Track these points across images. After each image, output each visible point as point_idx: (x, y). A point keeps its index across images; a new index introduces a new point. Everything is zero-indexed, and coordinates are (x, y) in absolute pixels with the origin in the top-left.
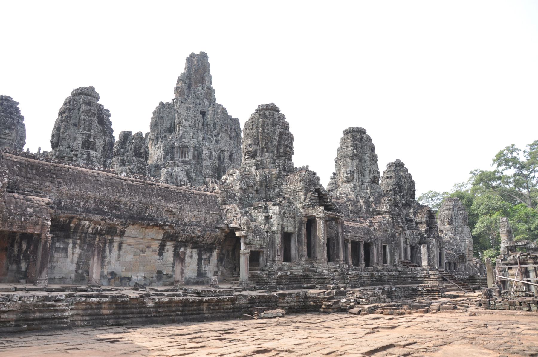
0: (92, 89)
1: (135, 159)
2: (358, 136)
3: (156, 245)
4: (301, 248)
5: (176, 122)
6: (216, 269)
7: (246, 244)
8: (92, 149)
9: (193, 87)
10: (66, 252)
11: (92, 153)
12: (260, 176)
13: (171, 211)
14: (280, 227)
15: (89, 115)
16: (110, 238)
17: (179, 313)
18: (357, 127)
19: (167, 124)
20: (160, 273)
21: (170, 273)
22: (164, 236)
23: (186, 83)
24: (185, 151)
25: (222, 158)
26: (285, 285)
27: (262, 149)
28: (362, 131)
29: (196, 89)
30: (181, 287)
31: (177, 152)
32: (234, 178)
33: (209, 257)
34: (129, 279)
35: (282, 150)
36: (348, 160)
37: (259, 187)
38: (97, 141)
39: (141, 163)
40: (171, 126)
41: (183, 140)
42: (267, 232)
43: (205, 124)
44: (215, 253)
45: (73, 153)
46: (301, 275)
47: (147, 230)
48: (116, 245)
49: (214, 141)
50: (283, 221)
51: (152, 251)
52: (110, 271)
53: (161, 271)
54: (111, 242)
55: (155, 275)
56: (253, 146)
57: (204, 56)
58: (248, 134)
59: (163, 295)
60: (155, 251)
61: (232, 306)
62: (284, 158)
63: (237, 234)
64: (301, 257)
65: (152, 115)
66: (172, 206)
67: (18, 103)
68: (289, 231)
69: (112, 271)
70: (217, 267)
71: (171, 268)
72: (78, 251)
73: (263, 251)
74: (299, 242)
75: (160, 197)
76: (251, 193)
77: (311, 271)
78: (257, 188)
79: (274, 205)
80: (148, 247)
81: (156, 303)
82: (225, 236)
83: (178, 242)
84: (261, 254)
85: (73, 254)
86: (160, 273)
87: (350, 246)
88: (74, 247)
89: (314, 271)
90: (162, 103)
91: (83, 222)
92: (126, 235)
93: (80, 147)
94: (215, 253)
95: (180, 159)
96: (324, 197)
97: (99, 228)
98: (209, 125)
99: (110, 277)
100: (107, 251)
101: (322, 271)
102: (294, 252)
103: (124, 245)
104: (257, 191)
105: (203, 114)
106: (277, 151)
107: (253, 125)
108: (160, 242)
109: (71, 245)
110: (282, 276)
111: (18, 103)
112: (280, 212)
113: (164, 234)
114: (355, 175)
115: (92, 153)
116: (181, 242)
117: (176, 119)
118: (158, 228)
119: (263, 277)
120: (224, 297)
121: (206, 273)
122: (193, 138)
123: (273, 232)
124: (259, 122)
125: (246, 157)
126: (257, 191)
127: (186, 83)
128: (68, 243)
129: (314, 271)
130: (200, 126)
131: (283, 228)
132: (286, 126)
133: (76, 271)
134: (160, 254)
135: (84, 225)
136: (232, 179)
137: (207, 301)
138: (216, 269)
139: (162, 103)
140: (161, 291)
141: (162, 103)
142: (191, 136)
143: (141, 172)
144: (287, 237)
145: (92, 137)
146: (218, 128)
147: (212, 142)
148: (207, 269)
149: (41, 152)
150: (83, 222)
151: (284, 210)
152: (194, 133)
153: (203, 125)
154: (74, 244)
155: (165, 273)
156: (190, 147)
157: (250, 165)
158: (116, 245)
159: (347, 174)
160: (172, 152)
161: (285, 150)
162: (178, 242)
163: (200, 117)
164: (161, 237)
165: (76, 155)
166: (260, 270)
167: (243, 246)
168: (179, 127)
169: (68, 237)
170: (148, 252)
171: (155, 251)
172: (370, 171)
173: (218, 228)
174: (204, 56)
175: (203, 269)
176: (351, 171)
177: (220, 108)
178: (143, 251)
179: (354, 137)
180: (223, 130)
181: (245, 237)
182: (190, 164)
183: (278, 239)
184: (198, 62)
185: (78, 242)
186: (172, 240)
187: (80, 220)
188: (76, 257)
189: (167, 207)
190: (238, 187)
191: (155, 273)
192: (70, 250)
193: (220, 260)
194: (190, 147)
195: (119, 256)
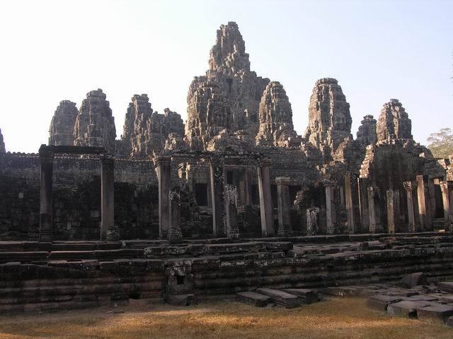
8: (98, 136)
14: (191, 181)
18: (324, 79)
28: (333, 82)
49: (238, 105)
57: (233, 26)
67: (75, 104)
111: (75, 104)
141: (196, 77)
146: (241, 93)
174: (233, 26)
184: (226, 33)
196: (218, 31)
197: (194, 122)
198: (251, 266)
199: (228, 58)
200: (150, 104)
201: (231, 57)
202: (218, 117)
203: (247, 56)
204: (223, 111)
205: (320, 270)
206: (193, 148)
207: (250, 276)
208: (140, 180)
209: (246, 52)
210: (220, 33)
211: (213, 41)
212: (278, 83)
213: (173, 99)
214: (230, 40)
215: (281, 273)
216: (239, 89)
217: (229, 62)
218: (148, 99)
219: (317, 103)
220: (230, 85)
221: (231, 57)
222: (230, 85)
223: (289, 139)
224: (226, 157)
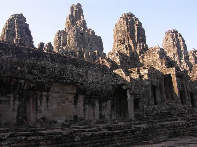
0: (22, 15)
2: (175, 35)
3: (72, 98)
4: (162, 96)
5: (68, 40)
6: (110, 113)
7: (131, 94)
10: (9, 104)
12: (130, 54)
13: (80, 74)
14: (150, 82)
16: (40, 93)
17: (99, 144)
20: (76, 117)
21: (83, 116)
22: (76, 91)
25: (94, 57)
26: (158, 119)
30: (94, 125)
32: (114, 55)
33: (106, 105)
34: (55, 122)
36: (171, 48)
37: (130, 60)
40: (65, 42)
42: (142, 86)
43: (84, 39)
44: (109, 103)
46: (166, 113)
47: (65, 87)
48: (44, 98)
49: (89, 48)
50: (151, 78)
51: (70, 102)
52: (41, 117)
53: (76, 116)
54: (41, 96)
55: (73, 119)
57: (79, 5)
58: (118, 31)
59: (85, 131)
60: (71, 102)
61: (133, 136)
63: (124, 87)
64: (163, 101)
66: (81, 71)
68: (155, 85)
69: (43, 117)
70: (111, 111)
71: (83, 113)
72: (17, 103)
73: (141, 99)
74: (161, 92)
75: (72, 65)
76: (125, 64)
77: (172, 109)
78: (129, 61)
79: (144, 68)
80: (66, 99)
81: (82, 138)
82: (115, 90)
83: (86, 95)
84: (140, 101)
85: (14, 105)
86: (76, 117)
87: (189, 94)
88: (14, 100)
89: (174, 109)
91: (20, 81)
92: (51, 90)
94: (109, 103)
96: (171, 63)
97: (32, 86)
98: (86, 40)
99: (42, 121)
100: (39, 102)
101: (180, 109)
102: (158, 99)
103: (50, 98)
104: (129, 63)
105: (82, 34)
107: (121, 25)
108: (74, 95)
109: (12, 99)
110: (156, 113)
112: (149, 72)
113: (77, 89)
114: (176, 56)
116: (88, 95)
118: (72, 85)
119: (143, 115)
120: (128, 130)
121: (105, 116)
123: (146, 86)
125: (119, 44)
126: (129, 63)
128: (10, 97)
129: (174, 109)
130: (81, 40)
131: (152, 83)
132: (140, 24)
133: (17, 118)
134: (75, 104)
135: (21, 83)
136: (113, 56)
137: (117, 134)
138: (110, 113)
139: (59, 30)
140: (82, 128)
144: (154, 88)
145: (23, 41)
146: (91, 41)
147: (88, 49)
148: (105, 113)
150: (20, 81)
151: (151, 72)
153: (82, 40)
154: (15, 97)
155: (79, 117)
158: (44, 98)
161: (142, 38)
162: (86, 95)
163: (80, 36)
164: (75, 91)
166: (140, 111)
167: (129, 96)
168: (70, 42)
169: (10, 93)
170: (67, 103)
171: (71, 102)
173: (110, 85)
175: (103, 113)
177: (91, 31)
178: (63, 102)
179: (172, 35)
180: (93, 42)
181: (130, 89)
183: (150, 90)
184: (76, 9)
185: (17, 96)
186: (82, 94)
187: (17, 79)
188: (16, 107)
189: (77, 71)
191: (72, 117)
192: (11, 102)
193: (113, 107)
195: (47, 106)
196: (71, 7)
197: (124, 40)
199: (79, 22)
201: (80, 22)
206: (131, 57)
208: (102, 80)
210: (72, 8)
211: (69, 12)
214: (76, 14)
216: (89, 39)
217: (79, 24)
219: (174, 43)
221: (80, 22)
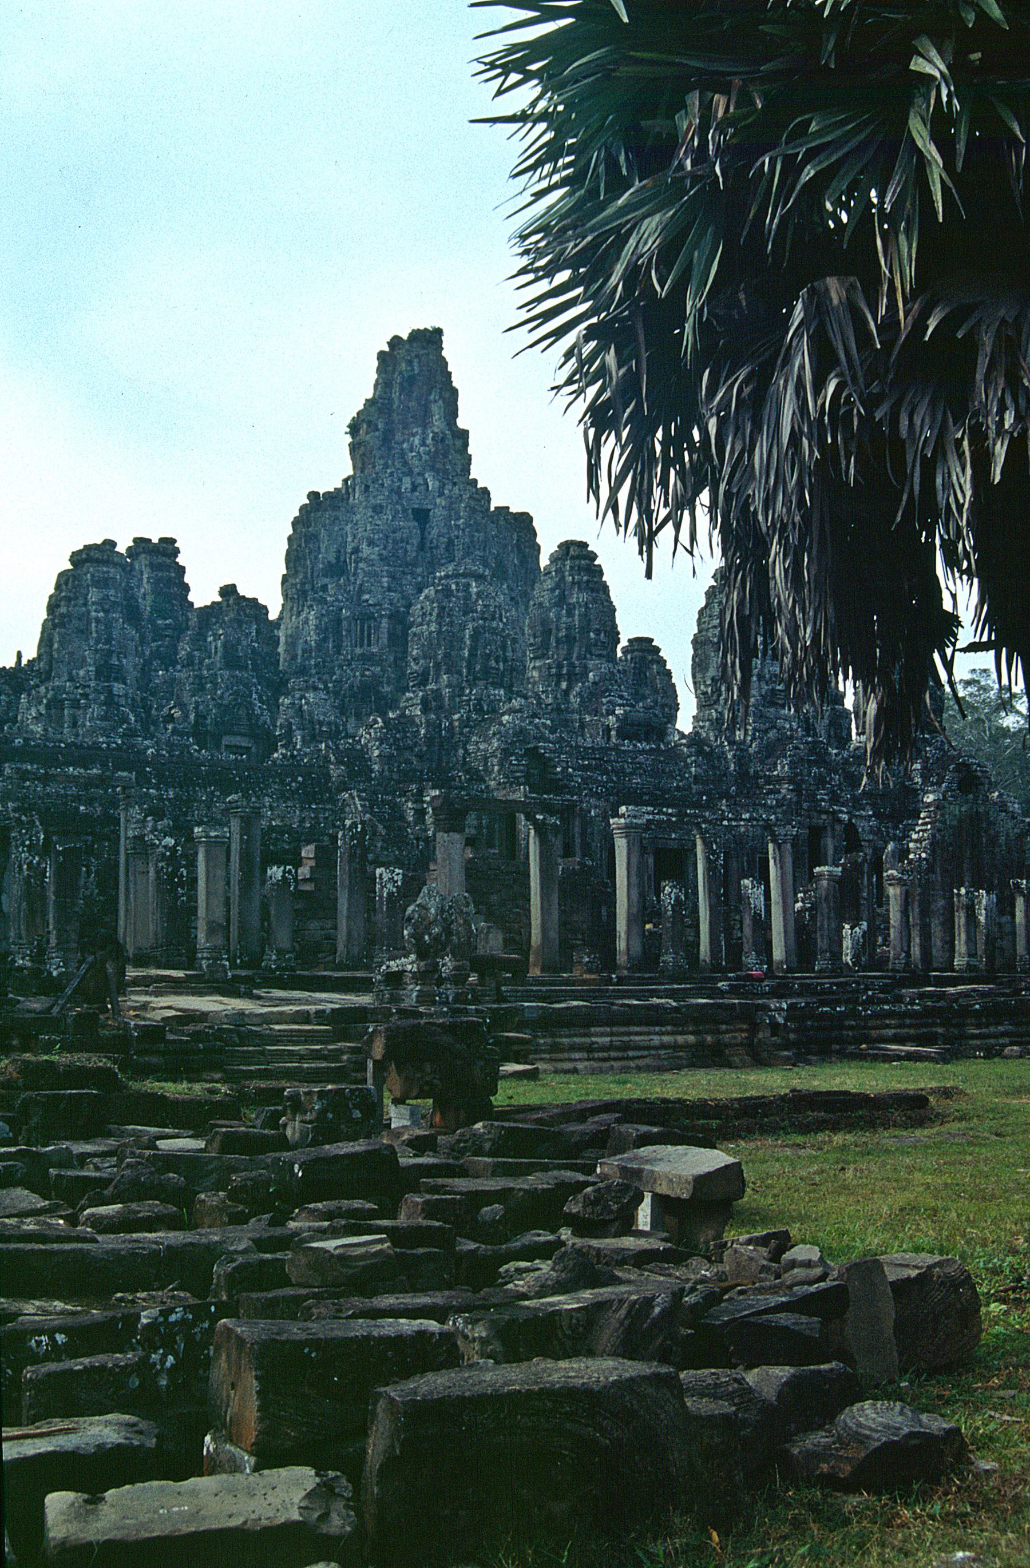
1: (226, 673)
8: (116, 680)
9: (398, 437)
11: (118, 688)
15: (107, 607)
19: (327, 554)
23: (378, 430)
24: (369, 627)
27: (437, 665)
29: (405, 446)
31: (349, 631)
35: (478, 667)
37: (425, 749)
38: (124, 661)
39: (239, 681)
40: (338, 558)
41: (366, 597)
42: (418, 839)
45: (80, 691)
56: (422, 662)
62: (481, 683)
65: (290, 531)
90: (313, 495)
93: (93, 677)
95: (358, 651)
98: (437, 547)
106: (469, 668)
115: (118, 688)
117: (349, 539)
122: (389, 590)
124: (432, 609)
127: (378, 430)
141: (313, 495)
142: (386, 585)
143: (240, 704)
149: (24, 662)
152: (393, 578)
156: (382, 616)
157: (415, 701)
159: (706, 686)
160: (338, 633)
165: (85, 696)
172: (760, 677)
174: (429, 340)
176: (713, 679)
182: (380, 662)
190: (376, 753)
194: (382, 616)
196: (381, 355)
198: (854, 1014)
200: (182, 570)
202: (493, 663)
203: (464, 434)
204: (504, 647)
205: (934, 1024)
207: (852, 1028)
209: (461, 423)
212: (585, 545)
213: (237, 554)
215: (888, 1026)
216: (450, 542)
218: (177, 552)
220: (423, 530)
222: (423, 530)
223: (619, 711)
224: (725, 823)
